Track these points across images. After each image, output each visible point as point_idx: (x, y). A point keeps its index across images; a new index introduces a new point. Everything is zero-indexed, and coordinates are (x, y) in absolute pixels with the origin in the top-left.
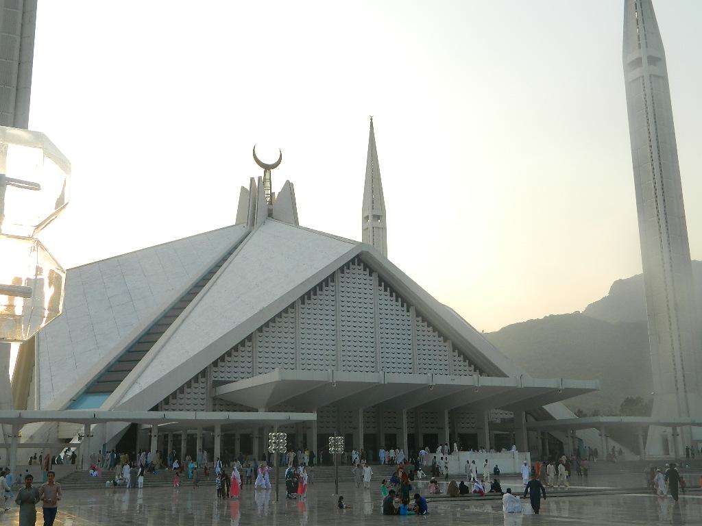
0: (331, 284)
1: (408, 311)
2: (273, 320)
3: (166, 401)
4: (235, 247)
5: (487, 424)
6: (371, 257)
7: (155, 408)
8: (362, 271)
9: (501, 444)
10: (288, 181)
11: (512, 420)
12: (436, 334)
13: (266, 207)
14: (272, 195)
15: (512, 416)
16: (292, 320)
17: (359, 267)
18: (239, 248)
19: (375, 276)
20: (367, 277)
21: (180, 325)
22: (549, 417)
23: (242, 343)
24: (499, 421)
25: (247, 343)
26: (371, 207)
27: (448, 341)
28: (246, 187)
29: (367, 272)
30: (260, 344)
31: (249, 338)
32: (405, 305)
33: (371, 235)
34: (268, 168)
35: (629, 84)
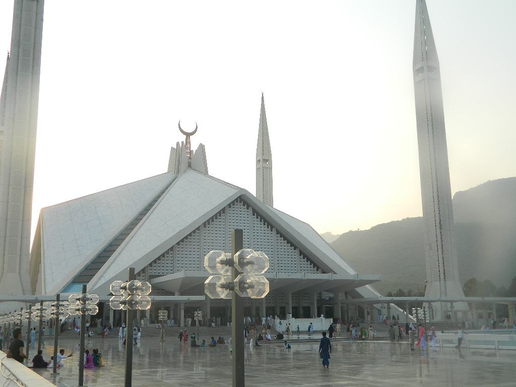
2: (186, 238)
4: (167, 188)
6: (248, 198)
10: (201, 144)
12: (289, 245)
13: (188, 160)
14: (191, 152)
16: (198, 238)
18: (166, 192)
19: (250, 210)
20: (246, 210)
22: (360, 296)
23: (167, 252)
24: (328, 299)
27: (297, 249)
29: (246, 207)
31: (172, 249)
33: (261, 172)
34: (188, 135)
35: (417, 84)
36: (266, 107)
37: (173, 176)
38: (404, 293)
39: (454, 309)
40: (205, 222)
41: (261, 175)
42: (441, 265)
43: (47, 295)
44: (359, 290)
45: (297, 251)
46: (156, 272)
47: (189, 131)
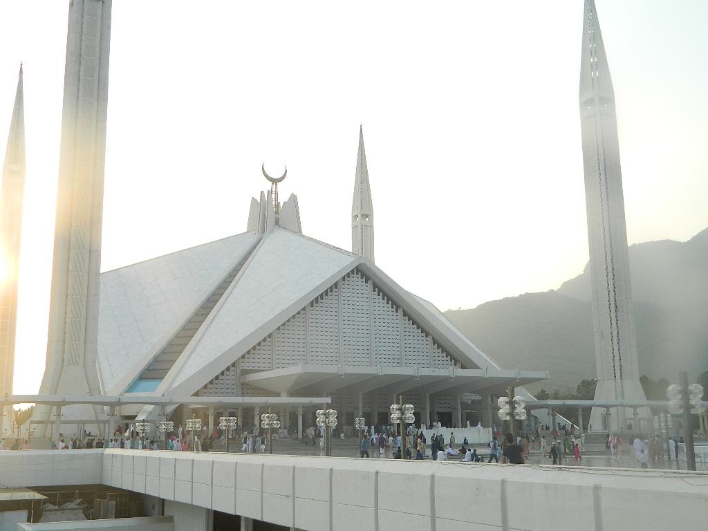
0: (334, 290)
1: (397, 311)
3: (205, 387)
4: (250, 253)
5: (459, 405)
7: (197, 394)
8: (359, 279)
10: (293, 194)
11: (479, 401)
13: (274, 216)
14: (278, 203)
15: (480, 398)
17: (358, 276)
23: (264, 340)
24: (469, 402)
25: (268, 339)
26: (360, 207)
28: (256, 200)
30: (278, 340)
31: (270, 336)
32: (395, 306)
34: (275, 181)
35: (584, 120)
36: (366, 148)
37: (256, 237)
40: (313, 301)
41: (360, 236)
42: (617, 358)
43: (109, 395)
47: (276, 176)
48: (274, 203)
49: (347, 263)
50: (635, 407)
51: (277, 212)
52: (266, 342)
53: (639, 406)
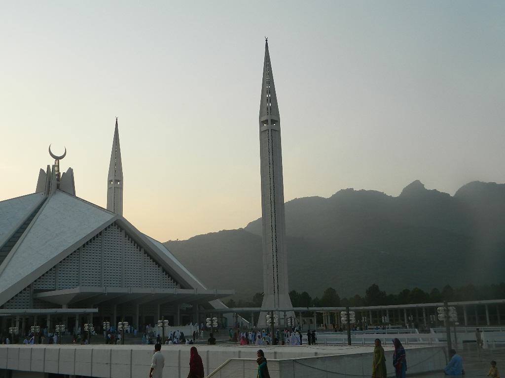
1: (140, 251)
5: (179, 311)
9: (185, 322)
10: (70, 168)
13: (56, 183)
14: (59, 173)
15: (192, 306)
19: (123, 232)
21: (12, 257)
24: (185, 309)
26: (114, 174)
31: (54, 267)
33: (113, 192)
34: (58, 159)
37: (43, 197)
38: (234, 303)
39: (287, 317)
44: (211, 303)
45: (160, 268)
46: (40, 287)
48: (56, 173)
49: (109, 218)
50: (285, 311)
51: (58, 180)
52: (54, 271)
53: (288, 311)
